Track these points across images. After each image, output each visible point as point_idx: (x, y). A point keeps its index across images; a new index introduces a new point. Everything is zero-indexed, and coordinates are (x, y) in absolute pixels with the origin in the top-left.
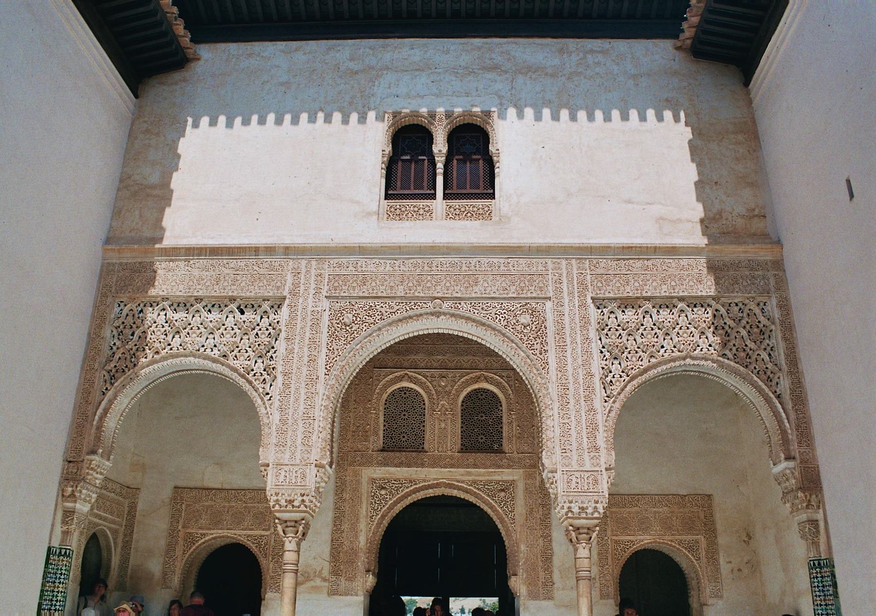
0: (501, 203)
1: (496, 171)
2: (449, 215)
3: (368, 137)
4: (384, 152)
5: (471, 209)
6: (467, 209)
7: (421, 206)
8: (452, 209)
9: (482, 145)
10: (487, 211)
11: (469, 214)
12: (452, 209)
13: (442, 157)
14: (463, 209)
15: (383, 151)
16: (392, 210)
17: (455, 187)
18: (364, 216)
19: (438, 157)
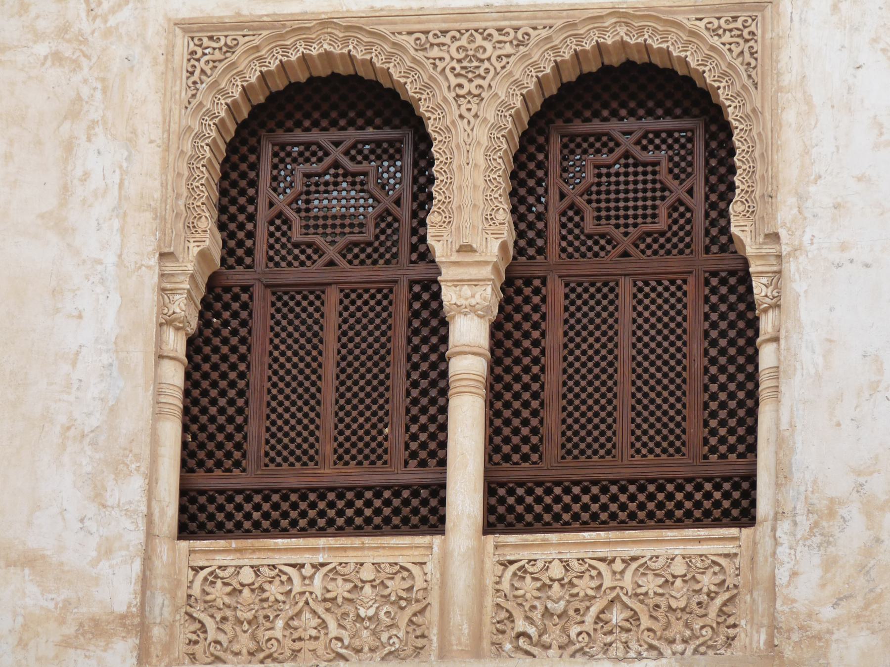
0: (783, 551)
1: (767, 357)
2: (511, 618)
3: (86, 177)
4: (170, 267)
5: (628, 581)
6: (608, 582)
7: (367, 573)
8: (529, 586)
9: (700, 189)
10: (711, 595)
11: (616, 616)
12: (529, 586)
13: (474, 282)
14: (585, 586)
15: (162, 255)
16: (218, 592)
17: (553, 448)
18: (66, 643)
19: (458, 282)
